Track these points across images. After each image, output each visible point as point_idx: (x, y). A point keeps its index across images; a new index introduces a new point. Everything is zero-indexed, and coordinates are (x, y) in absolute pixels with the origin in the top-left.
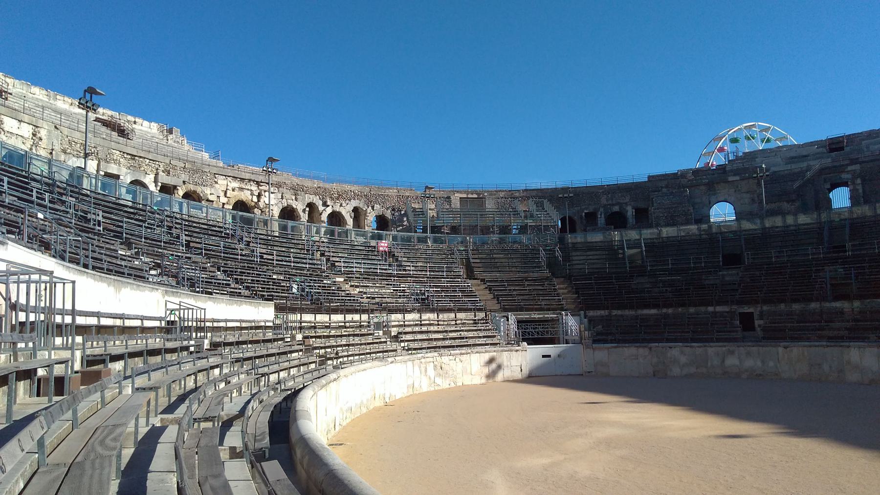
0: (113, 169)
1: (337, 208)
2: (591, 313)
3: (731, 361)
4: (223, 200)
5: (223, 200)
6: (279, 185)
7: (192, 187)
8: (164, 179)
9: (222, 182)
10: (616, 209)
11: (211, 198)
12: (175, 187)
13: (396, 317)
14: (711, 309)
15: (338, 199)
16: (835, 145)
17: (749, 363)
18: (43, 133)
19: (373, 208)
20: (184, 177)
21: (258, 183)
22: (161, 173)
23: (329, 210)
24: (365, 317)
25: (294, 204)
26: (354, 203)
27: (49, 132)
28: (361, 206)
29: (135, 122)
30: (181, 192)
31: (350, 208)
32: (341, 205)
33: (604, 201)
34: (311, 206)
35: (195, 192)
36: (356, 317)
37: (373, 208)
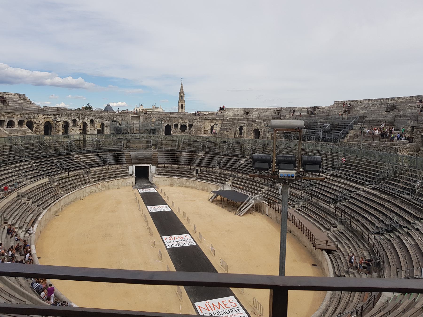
2: (159, 165)
3: (188, 183)
7: (30, 120)
9: (40, 116)
10: (184, 124)
11: (36, 122)
14: (190, 167)
16: (247, 112)
17: (191, 184)
24: (81, 171)
25: (68, 120)
26: (91, 118)
30: (26, 122)
31: (89, 120)
33: (180, 121)
35: (31, 121)
36: (79, 171)
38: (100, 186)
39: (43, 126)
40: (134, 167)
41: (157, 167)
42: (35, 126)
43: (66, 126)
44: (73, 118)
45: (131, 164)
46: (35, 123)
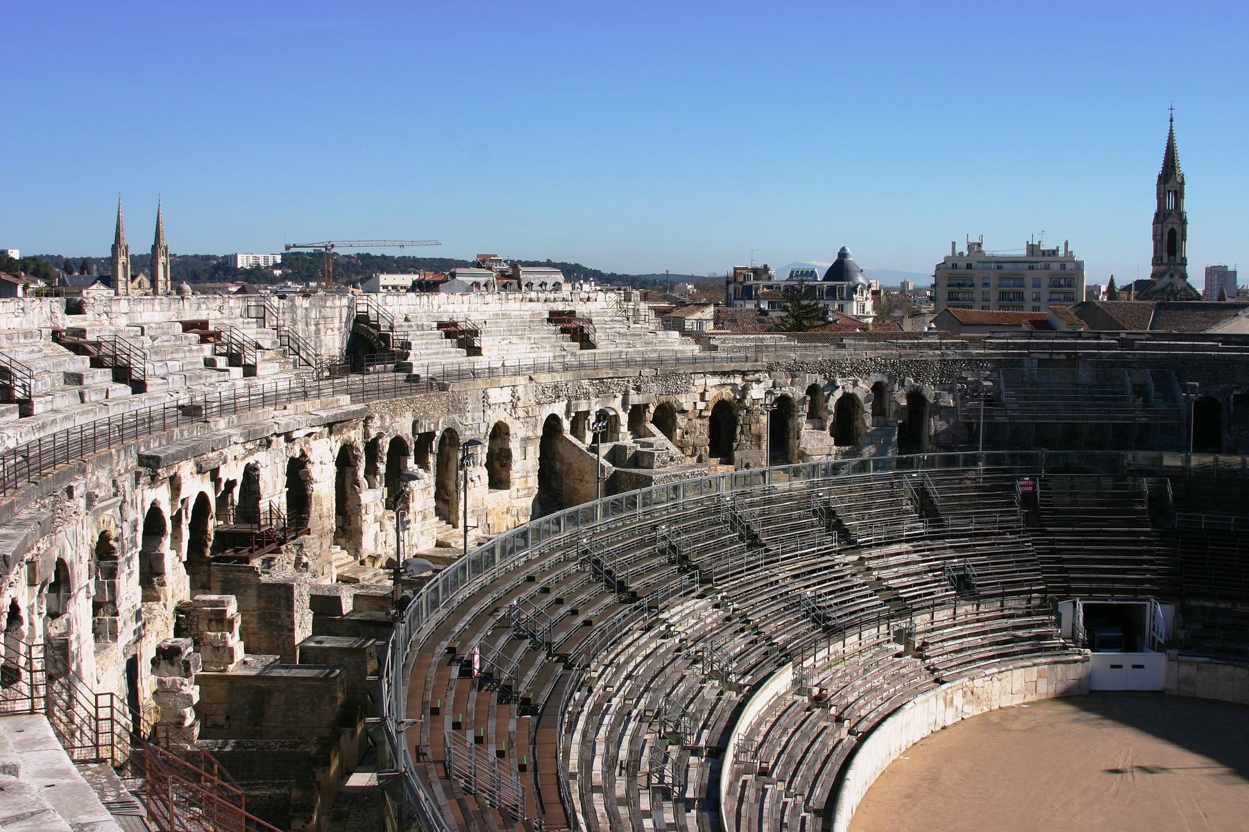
0: (583, 407)
1: (850, 390)
4: (701, 406)
5: (701, 406)
6: (770, 370)
7: (663, 399)
8: (635, 399)
9: (699, 381)
11: (685, 407)
12: (646, 406)
13: (921, 621)
15: (850, 374)
18: (520, 390)
19: (902, 384)
20: (655, 388)
21: (744, 374)
22: (632, 392)
23: (838, 394)
26: (875, 377)
27: (525, 386)
28: (886, 380)
29: (588, 299)
30: (652, 409)
32: (855, 384)
34: (813, 390)
37: (902, 384)
38: (958, 700)
39: (706, 422)
40: (1080, 604)
41: (1184, 613)
42: (681, 420)
43: (782, 411)
44: (809, 379)
45: (1067, 593)
46: (683, 412)
